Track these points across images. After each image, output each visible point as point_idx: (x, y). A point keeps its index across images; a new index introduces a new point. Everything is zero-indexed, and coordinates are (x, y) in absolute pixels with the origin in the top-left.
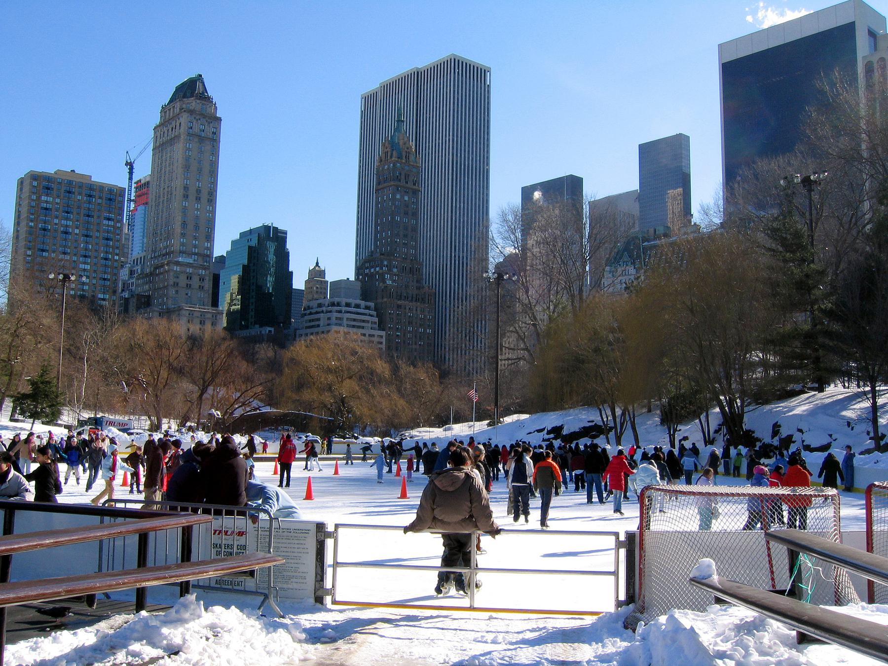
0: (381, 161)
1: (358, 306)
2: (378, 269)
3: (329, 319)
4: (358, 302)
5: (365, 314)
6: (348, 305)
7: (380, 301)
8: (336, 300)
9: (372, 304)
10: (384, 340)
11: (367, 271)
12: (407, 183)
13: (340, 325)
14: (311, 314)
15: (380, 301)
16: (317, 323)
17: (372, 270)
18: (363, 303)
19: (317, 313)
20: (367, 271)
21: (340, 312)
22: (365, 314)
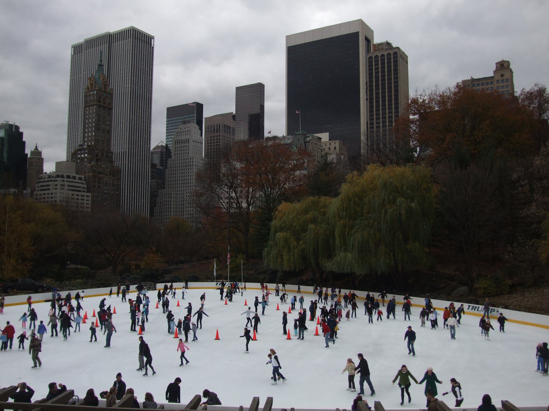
0: (88, 89)
1: (74, 178)
2: (86, 155)
3: (56, 185)
4: (74, 175)
5: (79, 183)
6: (68, 177)
7: (87, 174)
8: (60, 174)
9: (83, 177)
10: (90, 198)
11: (79, 156)
12: (104, 103)
13: (63, 189)
14: (44, 182)
15: (87, 174)
16: (48, 187)
17: (83, 156)
18: (77, 176)
19: (49, 181)
20: (79, 156)
21: (63, 181)
22: (79, 183)
